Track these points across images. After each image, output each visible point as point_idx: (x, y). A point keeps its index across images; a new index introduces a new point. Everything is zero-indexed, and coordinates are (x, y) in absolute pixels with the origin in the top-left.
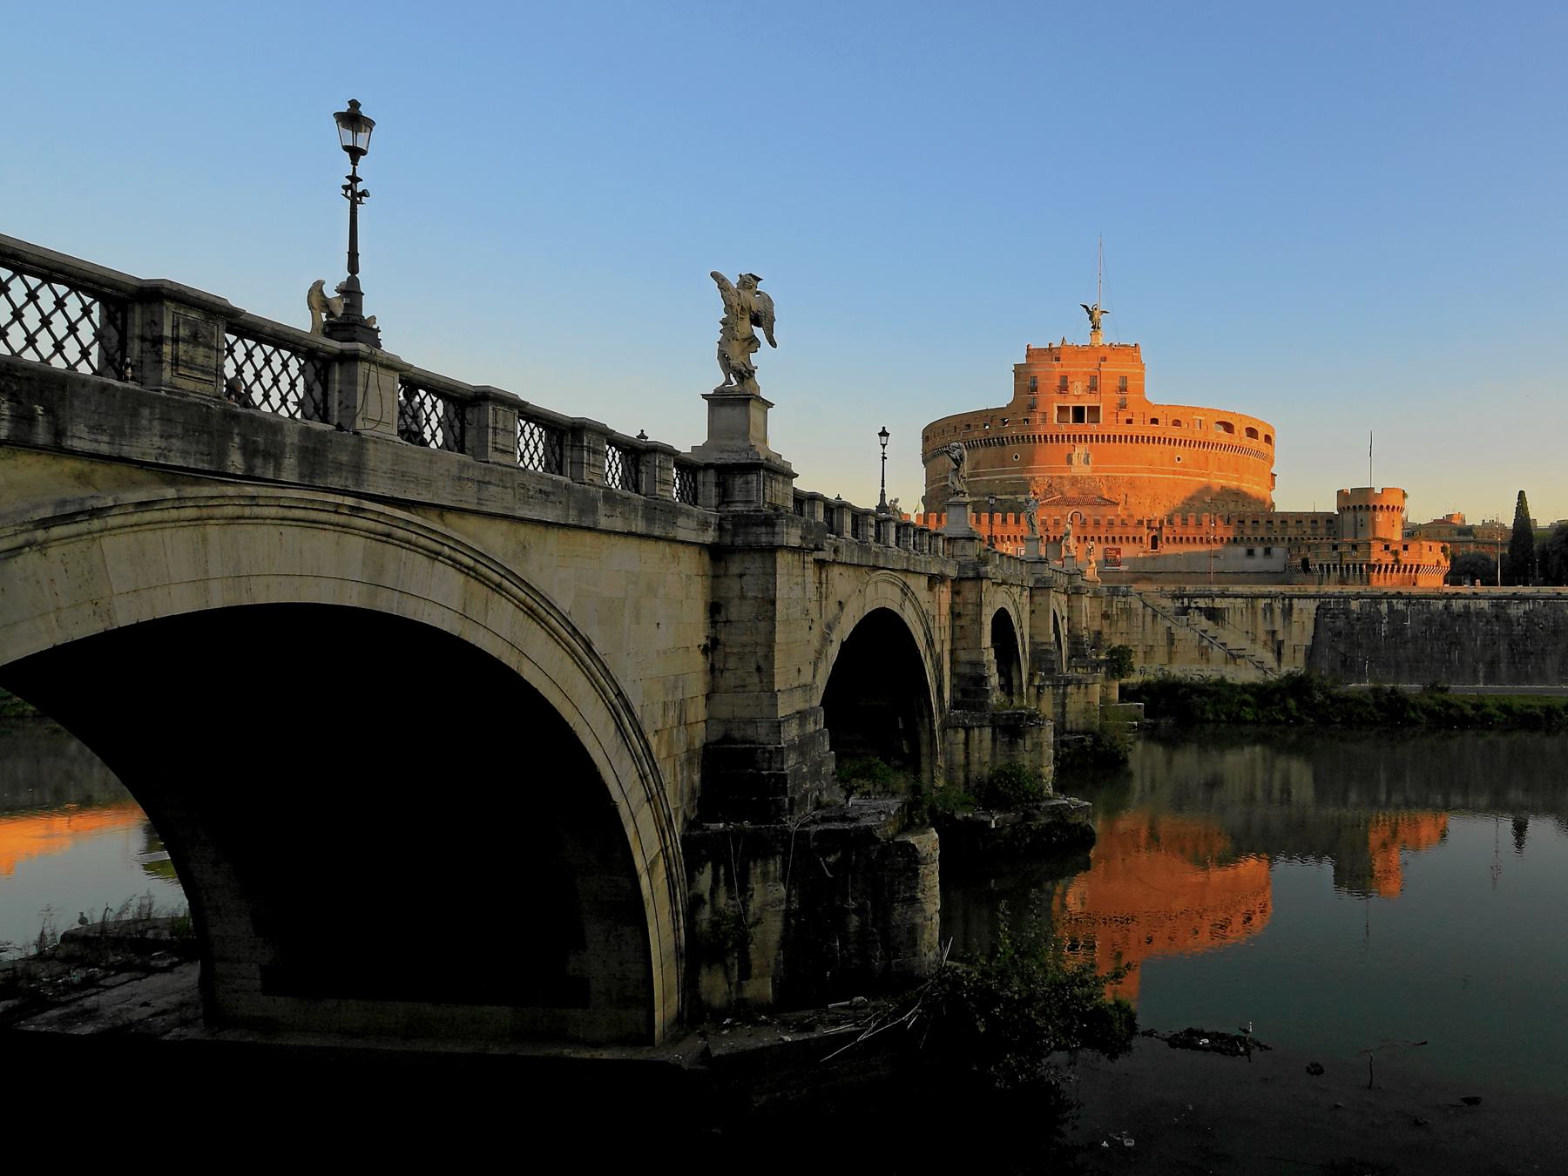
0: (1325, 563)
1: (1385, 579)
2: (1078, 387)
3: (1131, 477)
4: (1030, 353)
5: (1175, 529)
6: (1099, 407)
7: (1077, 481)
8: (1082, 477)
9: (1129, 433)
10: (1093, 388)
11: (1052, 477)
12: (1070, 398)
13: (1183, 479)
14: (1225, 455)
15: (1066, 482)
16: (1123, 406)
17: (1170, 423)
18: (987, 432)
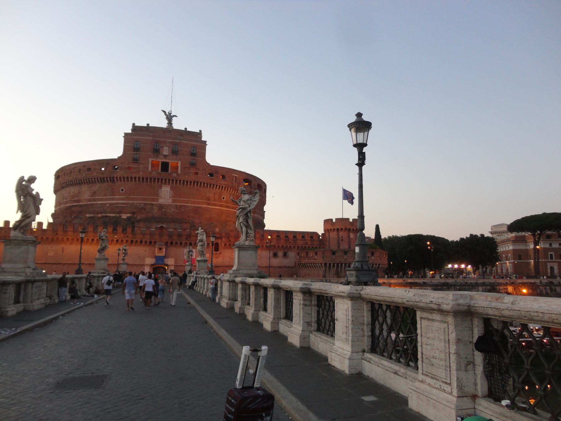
0: (328, 263)
2: (166, 151)
3: (197, 207)
4: (135, 128)
5: (230, 239)
10: (175, 153)
11: (145, 204)
12: (161, 156)
13: (226, 210)
15: (155, 208)
16: (193, 165)
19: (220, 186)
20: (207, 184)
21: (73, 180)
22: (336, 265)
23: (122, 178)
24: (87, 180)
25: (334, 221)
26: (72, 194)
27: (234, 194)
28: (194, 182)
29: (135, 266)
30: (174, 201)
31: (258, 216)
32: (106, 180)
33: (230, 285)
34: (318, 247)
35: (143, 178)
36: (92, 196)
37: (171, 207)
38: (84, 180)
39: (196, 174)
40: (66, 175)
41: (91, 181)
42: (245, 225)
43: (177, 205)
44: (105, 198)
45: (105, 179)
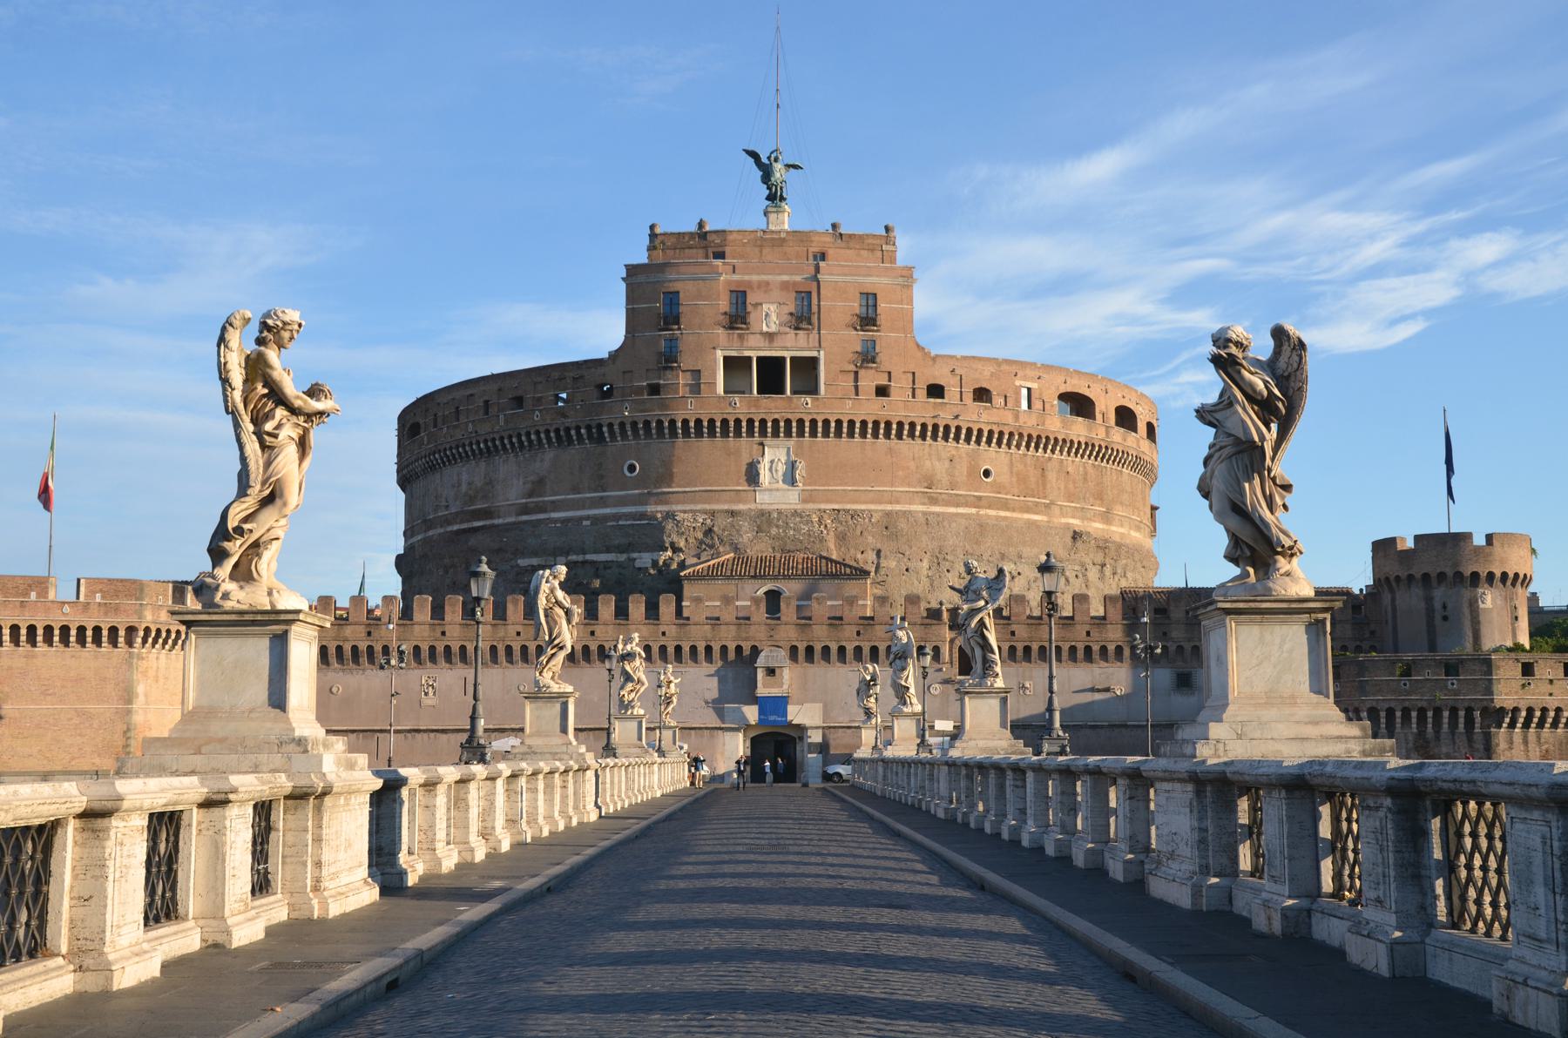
1: (1526, 742)
2: (770, 315)
3: (888, 514)
5: (1014, 627)
6: (814, 362)
7: (770, 522)
8: (780, 512)
9: (883, 415)
11: (713, 514)
12: (753, 340)
13: (997, 518)
14: (1074, 463)
15: (745, 525)
16: (868, 357)
17: (969, 397)
18: (562, 413)
19: (969, 431)
20: (924, 426)
21: (467, 443)
22: (1414, 714)
23: (628, 427)
24: (514, 440)
25: (1410, 544)
26: (464, 488)
27: (1025, 455)
28: (876, 424)
29: (693, 732)
30: (807, 498)
31: (1121, 530)
32: (575, 438)
33: (949, 772)
34: (1351, 645)
35: (699, 422)
36: (530, 496)
37: (798, 519)
38: (502, 439)
39: (882, 391)
40: (439, 420)
41: (526, 444)
42: (979, 644)
43: (820, 510)
44: (581, 498)
45: (573, 432)
